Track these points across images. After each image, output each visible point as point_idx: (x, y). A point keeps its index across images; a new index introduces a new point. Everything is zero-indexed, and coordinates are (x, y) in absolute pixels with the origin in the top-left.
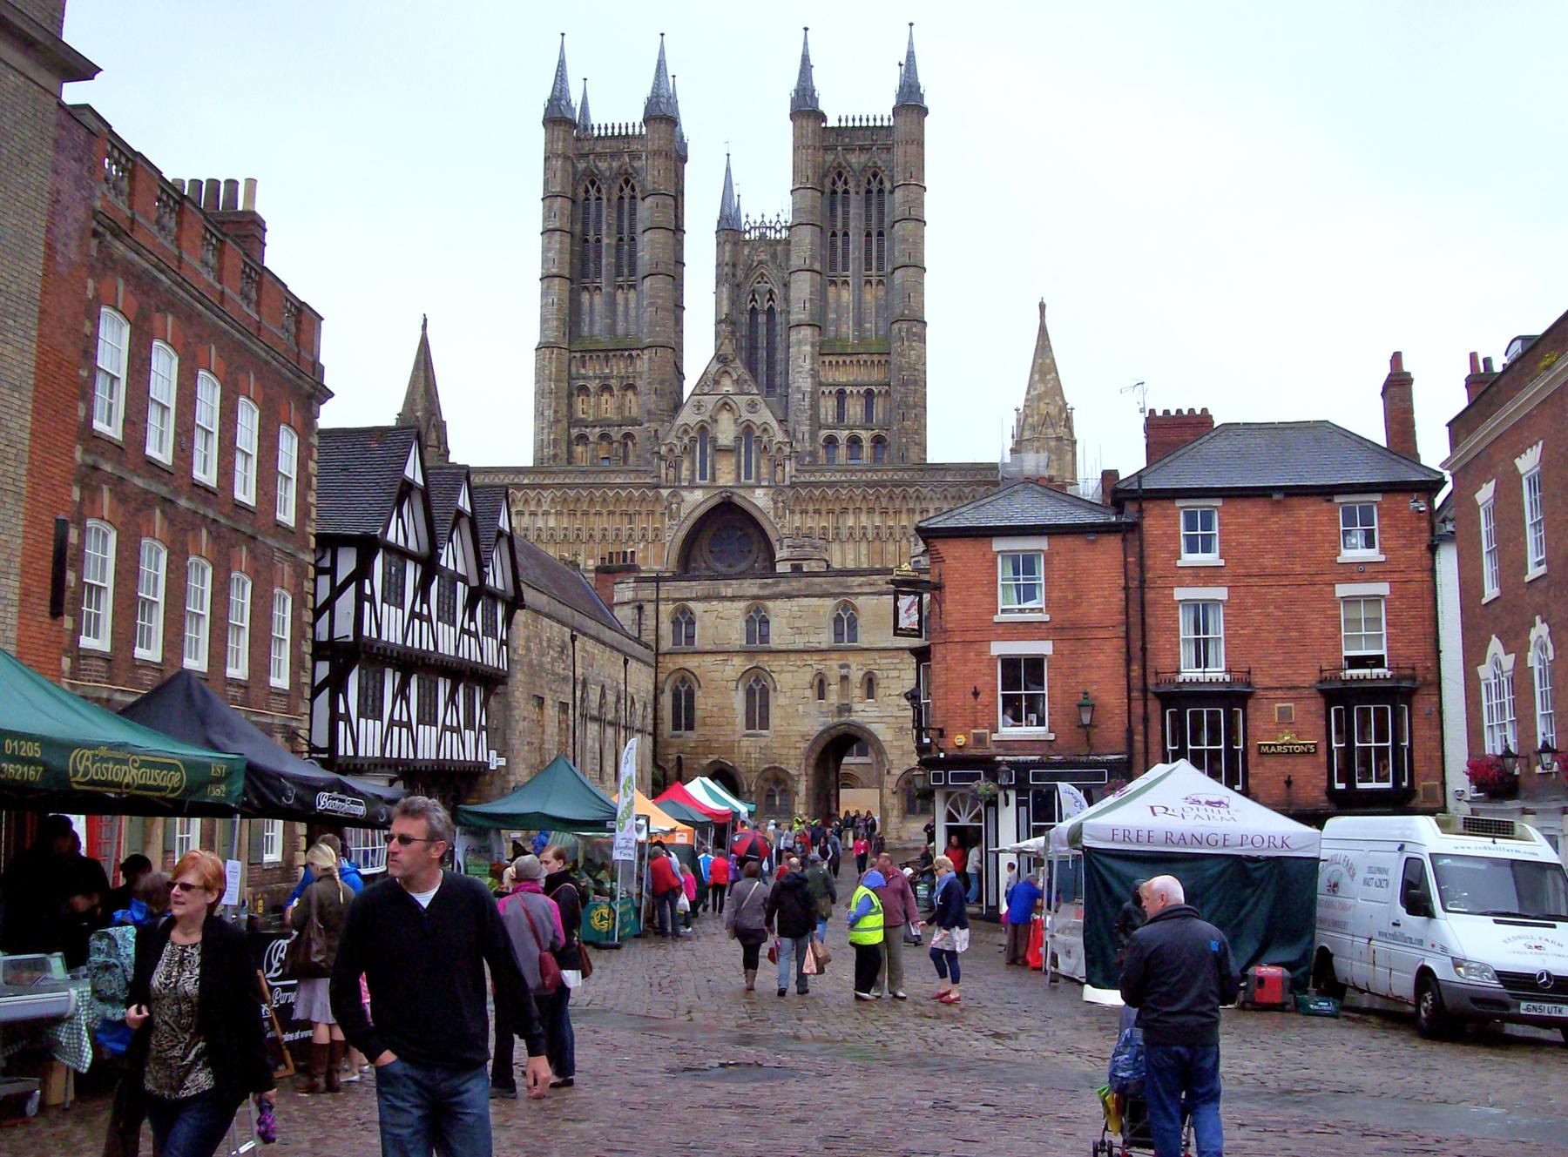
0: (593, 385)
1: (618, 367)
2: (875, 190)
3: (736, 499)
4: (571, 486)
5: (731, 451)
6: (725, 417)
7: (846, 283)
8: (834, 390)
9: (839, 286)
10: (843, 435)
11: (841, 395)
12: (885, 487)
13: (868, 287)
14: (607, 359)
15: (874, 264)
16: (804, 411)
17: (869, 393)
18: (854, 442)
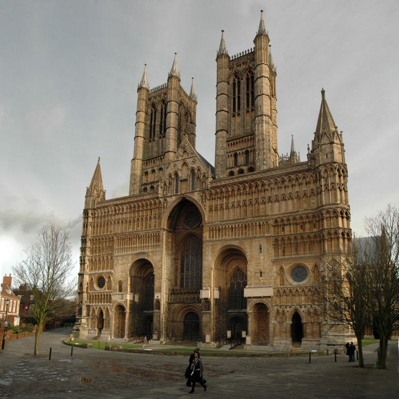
0: (149, 170)
1: (157, 163)
2: (250, 77)
3: (187, 198)
4: (132, 202)
5: (186, 180)
6: (185, 167)
7: (239, 114)
8: (232, 154)
9: (236, 116)
10: (236, 170)
11: (236, 155)
12: (247, 183)
13: (248, 114)
14: (154, 162)
15: (250, 104)
16: (220, 163)
17: (247, 152)
18: (241, 172)
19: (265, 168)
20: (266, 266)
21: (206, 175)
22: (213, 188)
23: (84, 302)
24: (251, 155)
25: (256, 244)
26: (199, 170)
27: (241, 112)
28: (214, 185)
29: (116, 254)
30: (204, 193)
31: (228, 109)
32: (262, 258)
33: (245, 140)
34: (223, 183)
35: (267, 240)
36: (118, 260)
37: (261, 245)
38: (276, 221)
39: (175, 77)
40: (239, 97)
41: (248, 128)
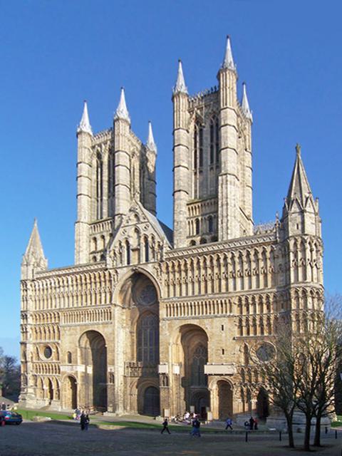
10: (198, 239)
12: (207, 255)
15: (215, 159)
18: (203, 241)
19: (230, 238)
20: (228, 344)
21: (161, 244)
22: (169, 259)
23: (29, 371)
24: (214, 221)
25: (217, 323)
26: (153, 238)
27: (204, 168)
28: (171, 256)
29: (62, 323)
30: (160, 265)
31: (188, 164)
32: (224, 335)
33: (208, 204)
34: (181, 254)
35: (230, 320)
36: (65, 331)
37: (223, 326)
38: (240, 300)
39: (122, 119)
40: (201, 150)
41: (212, 189)
